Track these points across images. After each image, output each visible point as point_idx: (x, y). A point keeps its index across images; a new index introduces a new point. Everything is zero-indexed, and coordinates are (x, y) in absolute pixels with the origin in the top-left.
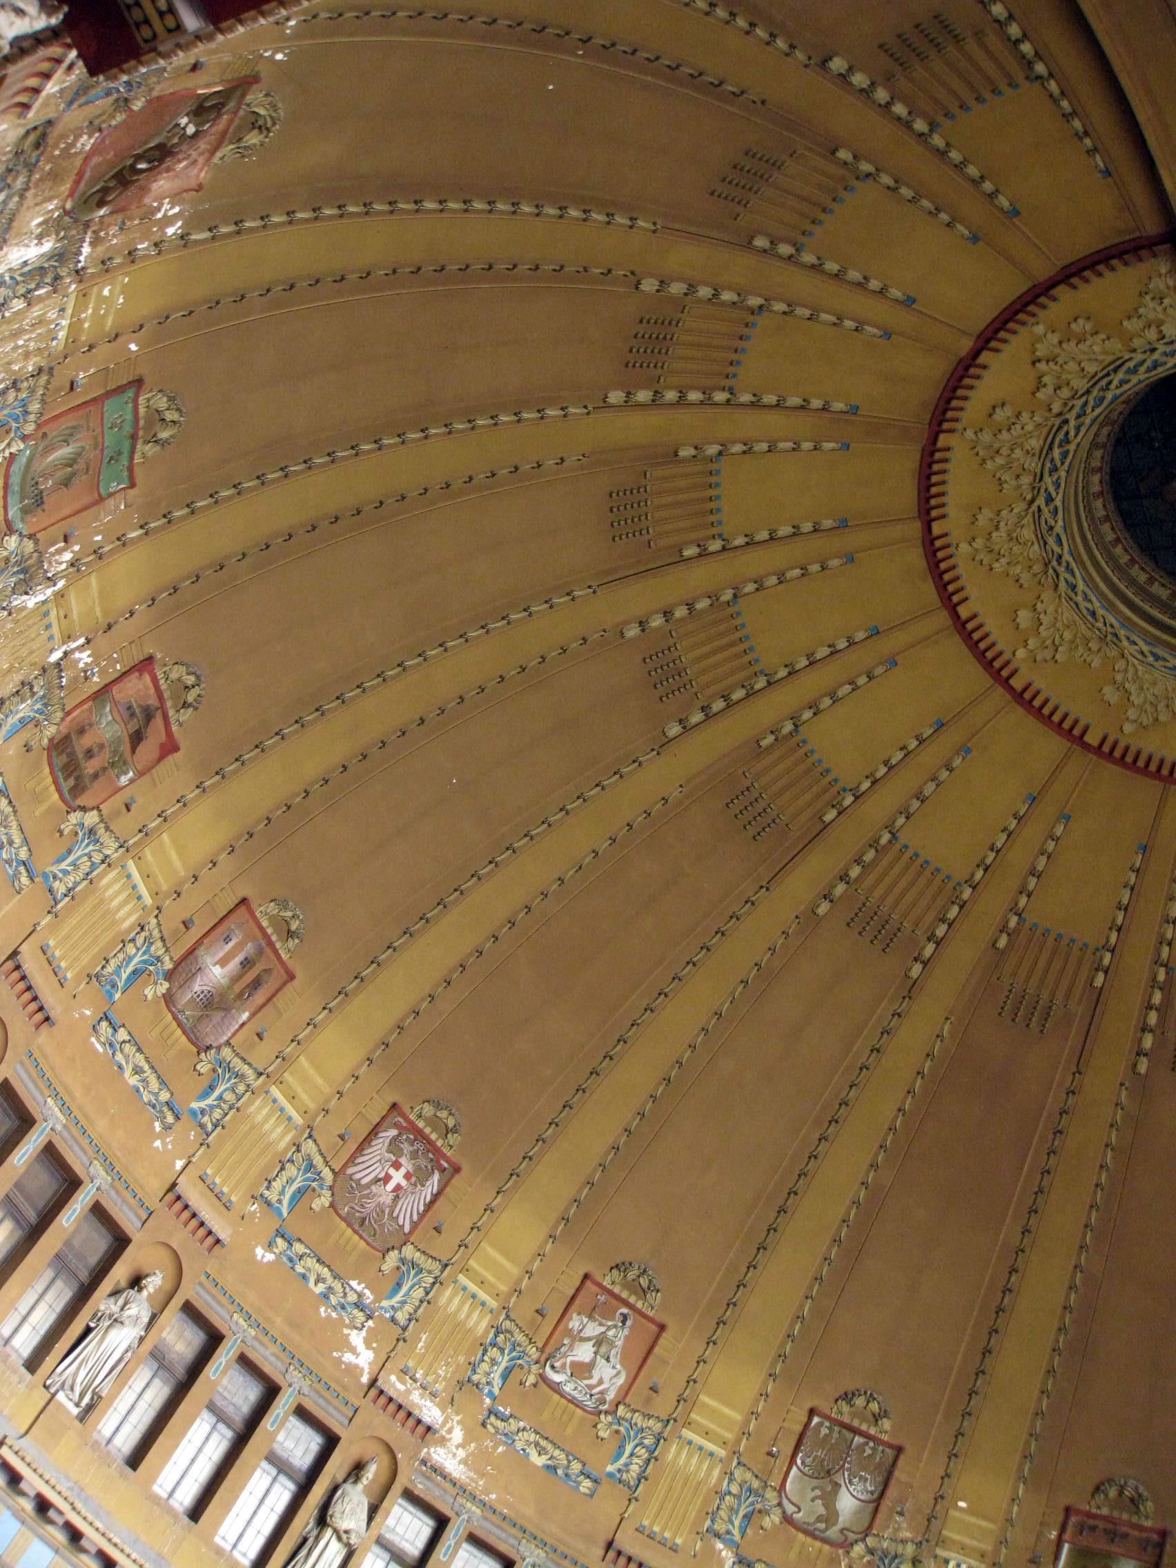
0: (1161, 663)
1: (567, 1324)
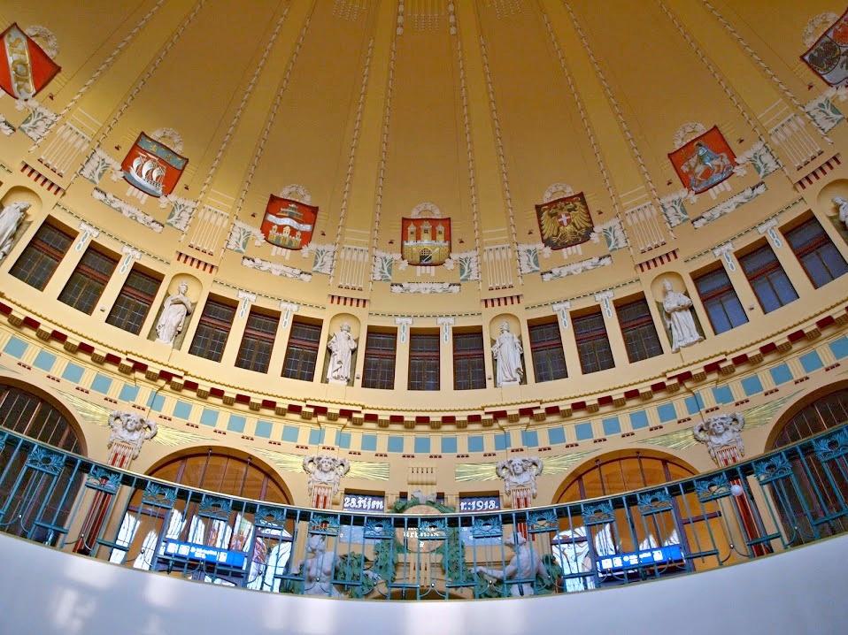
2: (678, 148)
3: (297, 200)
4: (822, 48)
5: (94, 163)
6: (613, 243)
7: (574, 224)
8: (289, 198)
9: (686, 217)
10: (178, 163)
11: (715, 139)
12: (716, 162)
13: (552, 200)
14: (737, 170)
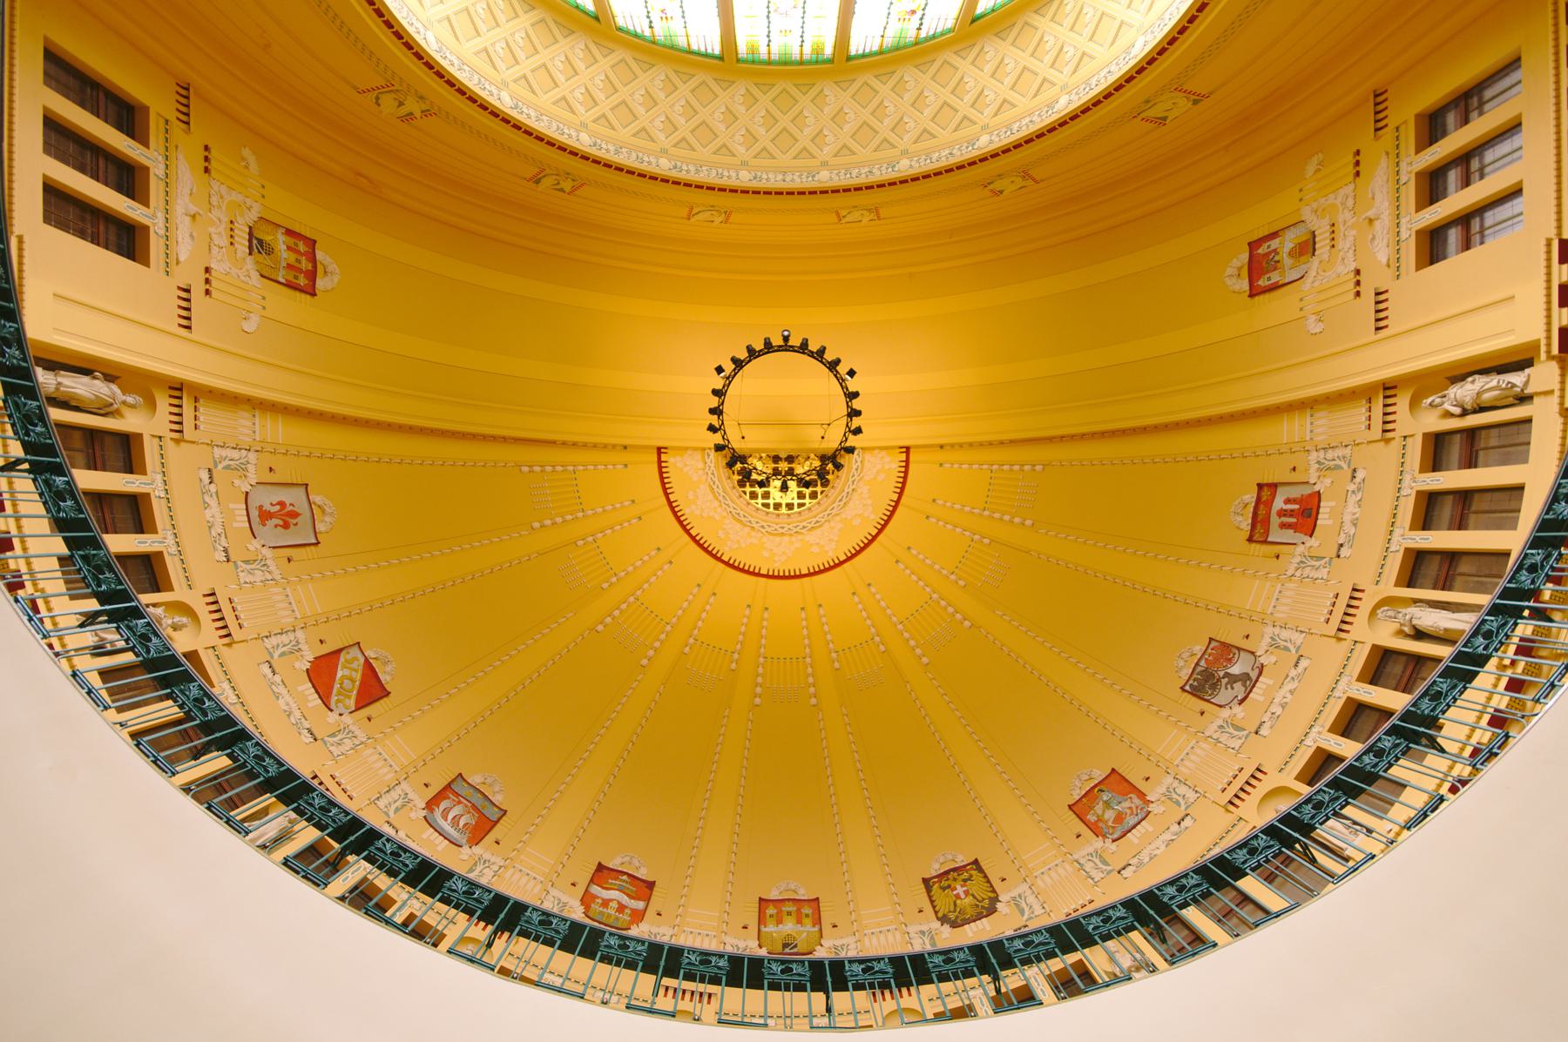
0: (844, 499)
1: (1093, 824)
2: (1077, 798)
3: (630, 872)
4: (1199, 677)
5: (394, 794)
6: (1027, 913)
7: (973, 895)
8: (620, 869)
9: (1109, 868)
10: (493, 814)
11: (1116, 781)
12: (1126, 804)
13: (942, 871)
14: (1151, 807)
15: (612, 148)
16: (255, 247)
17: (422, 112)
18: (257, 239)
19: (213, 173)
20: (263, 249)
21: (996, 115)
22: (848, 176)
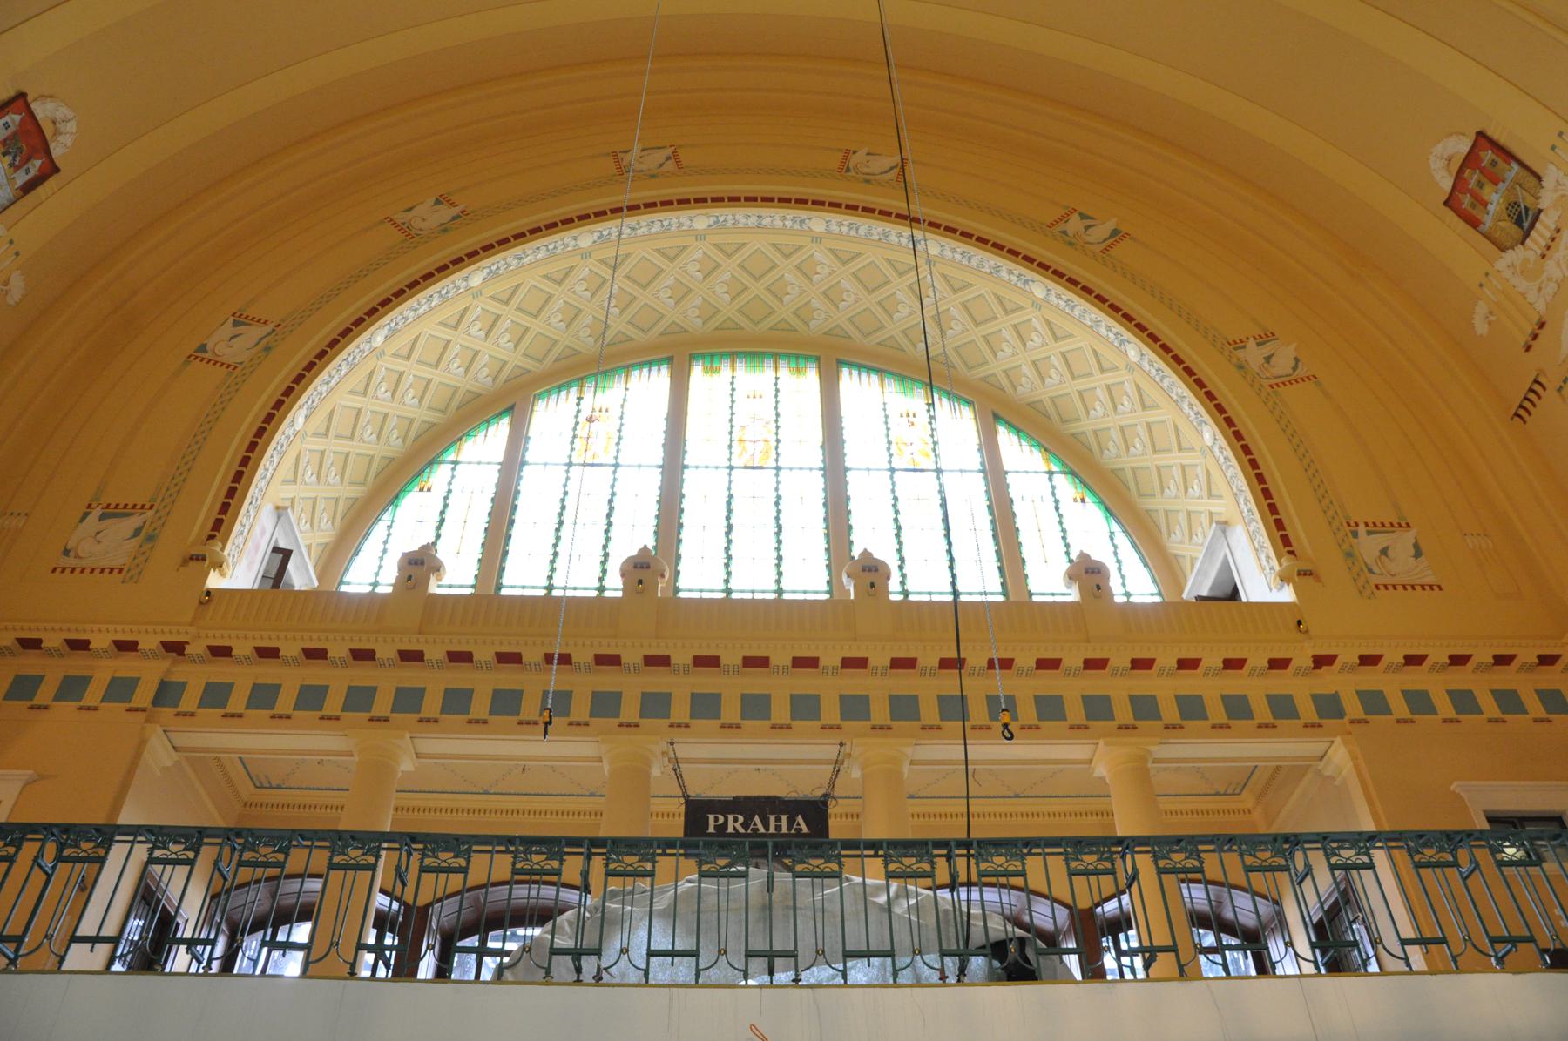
15: (1004, 275)
16: (1529, 218)
17: (1244, 347)
18: (1521, 227)
19: (1535, 319)
20: (1520, 212)
21: (465, 310)
22: (665, 223)
